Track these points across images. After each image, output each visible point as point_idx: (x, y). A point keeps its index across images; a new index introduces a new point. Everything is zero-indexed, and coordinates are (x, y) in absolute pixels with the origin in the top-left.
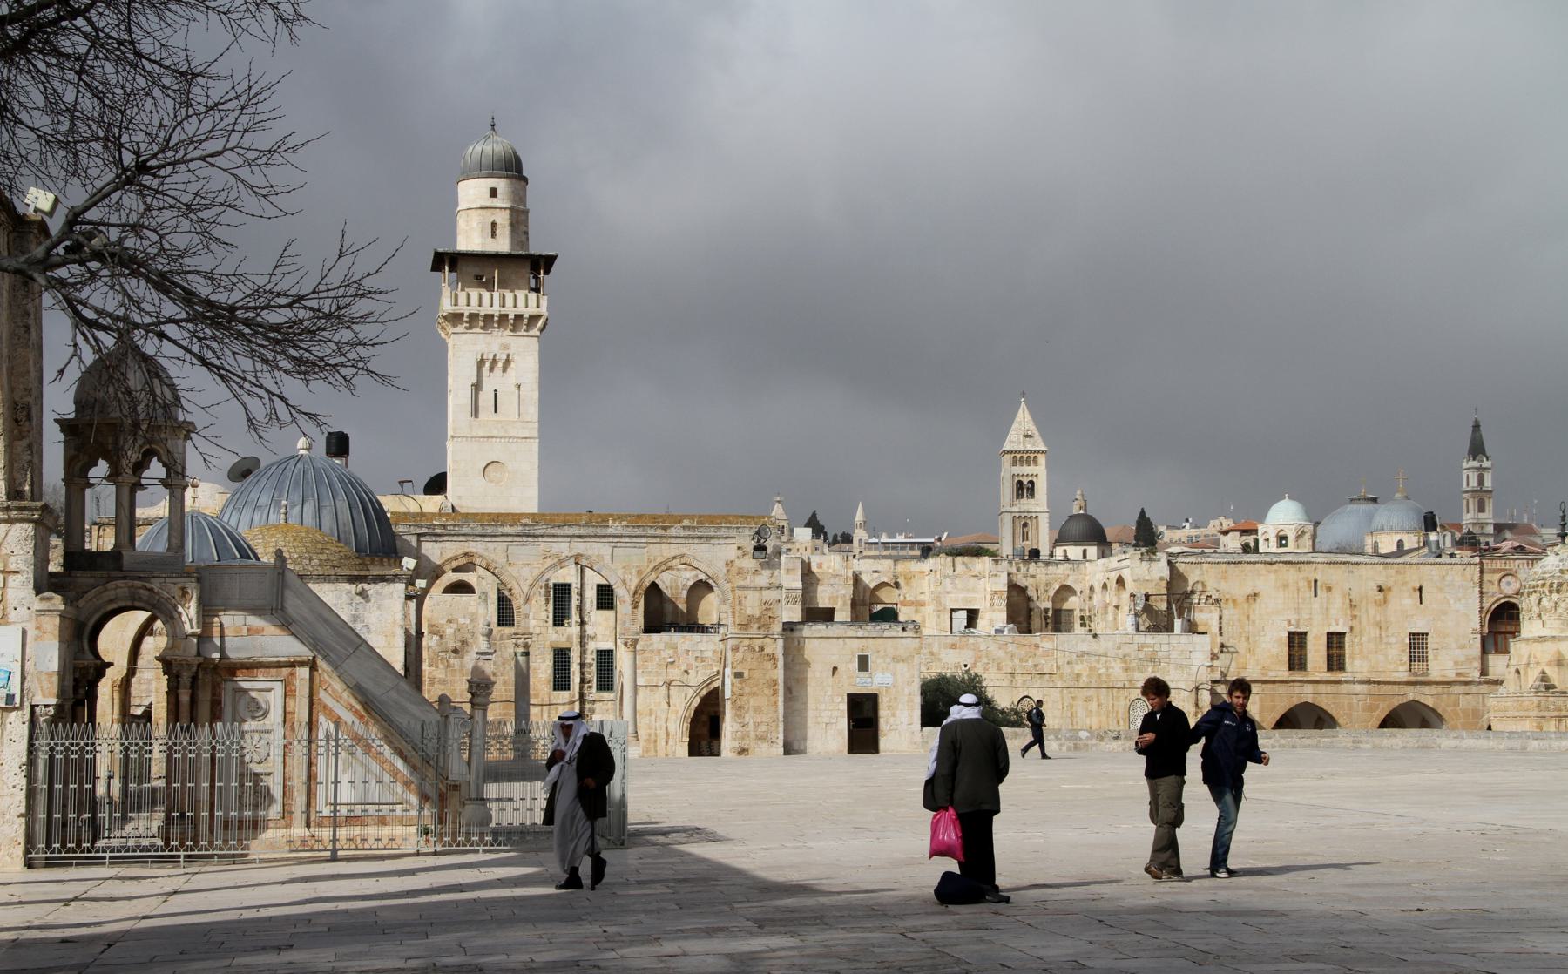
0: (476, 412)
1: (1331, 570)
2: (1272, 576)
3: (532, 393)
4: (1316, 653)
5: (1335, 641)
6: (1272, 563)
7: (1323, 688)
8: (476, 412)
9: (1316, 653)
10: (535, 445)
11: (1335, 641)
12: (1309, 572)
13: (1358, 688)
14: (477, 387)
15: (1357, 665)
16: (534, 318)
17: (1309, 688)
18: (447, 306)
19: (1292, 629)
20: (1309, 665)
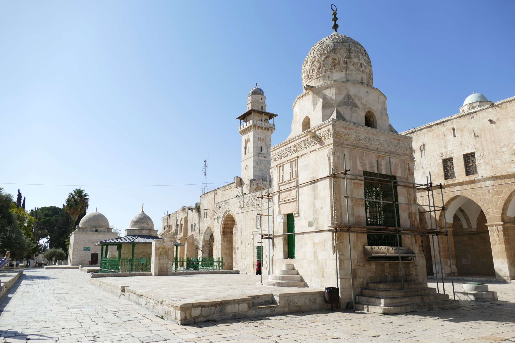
0: (245, 154)
1: (461, 120)
2: (431, 133)
3: (252, 145)
4: (459, 167)
5: (469, 159)
6: (430, 127)
7: (466, 187)
8: (245, 154)
9: (459, 167)
10: (252, 159)
11: (469, 159)
12: (449, 125)
13: (488, 183)
14: (245, 148)
15: (483, 170)
16: (251, 126)
17: (458, 188)
18: (240, 130)
19: (444, 157)
20: (456, 174)
